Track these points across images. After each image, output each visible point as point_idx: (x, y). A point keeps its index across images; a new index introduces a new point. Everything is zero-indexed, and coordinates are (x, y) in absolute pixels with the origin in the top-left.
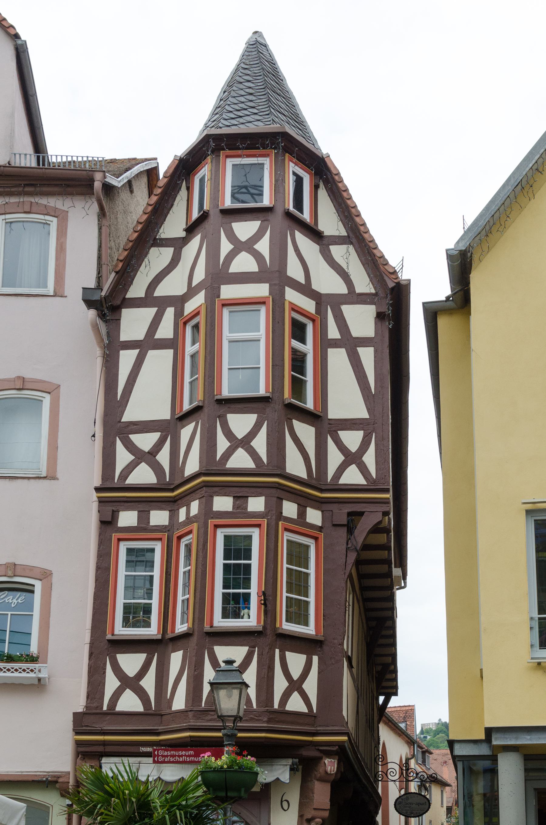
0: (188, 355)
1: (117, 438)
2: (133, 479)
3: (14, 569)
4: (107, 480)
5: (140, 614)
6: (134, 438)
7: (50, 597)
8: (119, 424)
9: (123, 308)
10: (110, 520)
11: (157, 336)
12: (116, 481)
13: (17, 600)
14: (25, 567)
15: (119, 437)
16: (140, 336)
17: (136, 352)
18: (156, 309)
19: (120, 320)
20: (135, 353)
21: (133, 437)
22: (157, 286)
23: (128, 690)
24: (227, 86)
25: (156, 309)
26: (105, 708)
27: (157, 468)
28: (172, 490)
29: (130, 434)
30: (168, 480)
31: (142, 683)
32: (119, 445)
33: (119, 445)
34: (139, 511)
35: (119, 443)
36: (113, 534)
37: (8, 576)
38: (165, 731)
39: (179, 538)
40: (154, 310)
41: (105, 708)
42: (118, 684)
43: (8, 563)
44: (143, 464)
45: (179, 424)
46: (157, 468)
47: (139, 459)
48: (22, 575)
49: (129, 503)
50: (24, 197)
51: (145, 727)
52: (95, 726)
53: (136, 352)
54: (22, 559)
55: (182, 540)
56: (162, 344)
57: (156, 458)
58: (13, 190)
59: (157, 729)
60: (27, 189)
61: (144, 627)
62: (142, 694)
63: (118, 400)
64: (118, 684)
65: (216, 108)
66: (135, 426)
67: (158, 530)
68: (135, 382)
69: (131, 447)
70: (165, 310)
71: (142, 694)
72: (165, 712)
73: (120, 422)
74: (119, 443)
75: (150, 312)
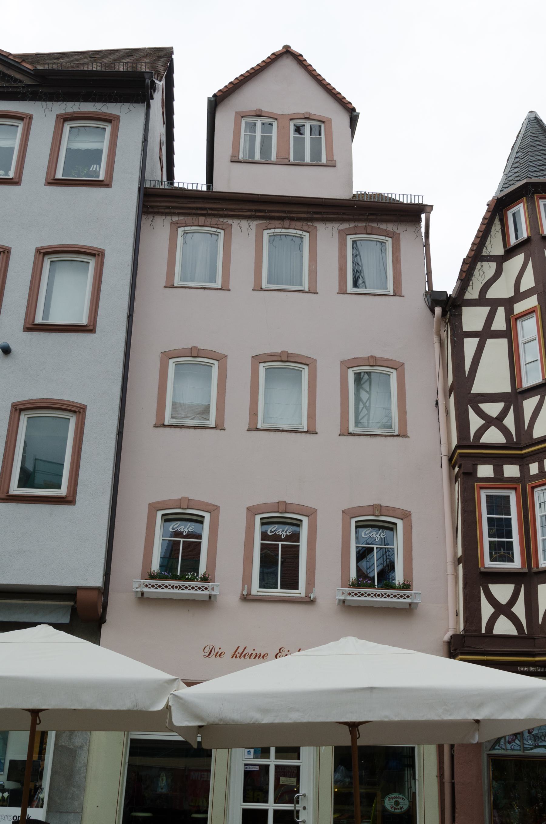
0: (522, 343)
1: (469, 406)
2: (486, 439)
3: (381, 510)
4: (464, 440)
5: (501, 550)
6: (483, 406)
7: (411, 533)
8: (470, 395)
9: (463, 307)
10: (472, 472)
11: (493, 328)
12: (471, 440)
13: (379, 536)
14: (389, 508)
15: (470, 406)
16: (479, 327)
17: (477, 340)
18: (489, 308)
19: (461, 315)
20: (475, 341)
21: (481, 405)
22: (487, 291)
23: (502, 616)
24: (519, 148)
25: (489, 308)
26: (483, 631)
27: (505, 431)
28: (521, 449)
29: (479, 403)
30: (515, 441)
31: (514, 610)
32: (471, 412)
33: (471, 412)
34: (493, 465)
35: (471, 411)
36: (476, 484)
37: (376, 516)
38: (543, 653)
39: (533, 488)
40: (488, 308)
41: (483, 631)
42: (493, 610)
43: (376, 505)
44: (493, 428)
45: (519, 397)
46: (505, 431)
47: (489, 423)
48: (387, 515)
49: (485, 459)
50: (369, 222)
51: (521, 649)
52: (476, 647)
53: (477, 340)
54: (386, 502)
55: (535, 490)
56: (498, 334)
57: (503, 422)
58: (360, 217)
59: (534, 651)
60: (370, 217)
61: (508, 562)
62: (514, 619)
63: (466, 376)
64: (493, 610)
65: (513, 163)
66: (482, 397)
67: (512, 481)
68: (479, 363)
69: (481, 414)
70: (497, 308)
71: (514, 619)
72: (539, 636)
73: (470, 393)
74: (471, 411)
75: (485, 310)
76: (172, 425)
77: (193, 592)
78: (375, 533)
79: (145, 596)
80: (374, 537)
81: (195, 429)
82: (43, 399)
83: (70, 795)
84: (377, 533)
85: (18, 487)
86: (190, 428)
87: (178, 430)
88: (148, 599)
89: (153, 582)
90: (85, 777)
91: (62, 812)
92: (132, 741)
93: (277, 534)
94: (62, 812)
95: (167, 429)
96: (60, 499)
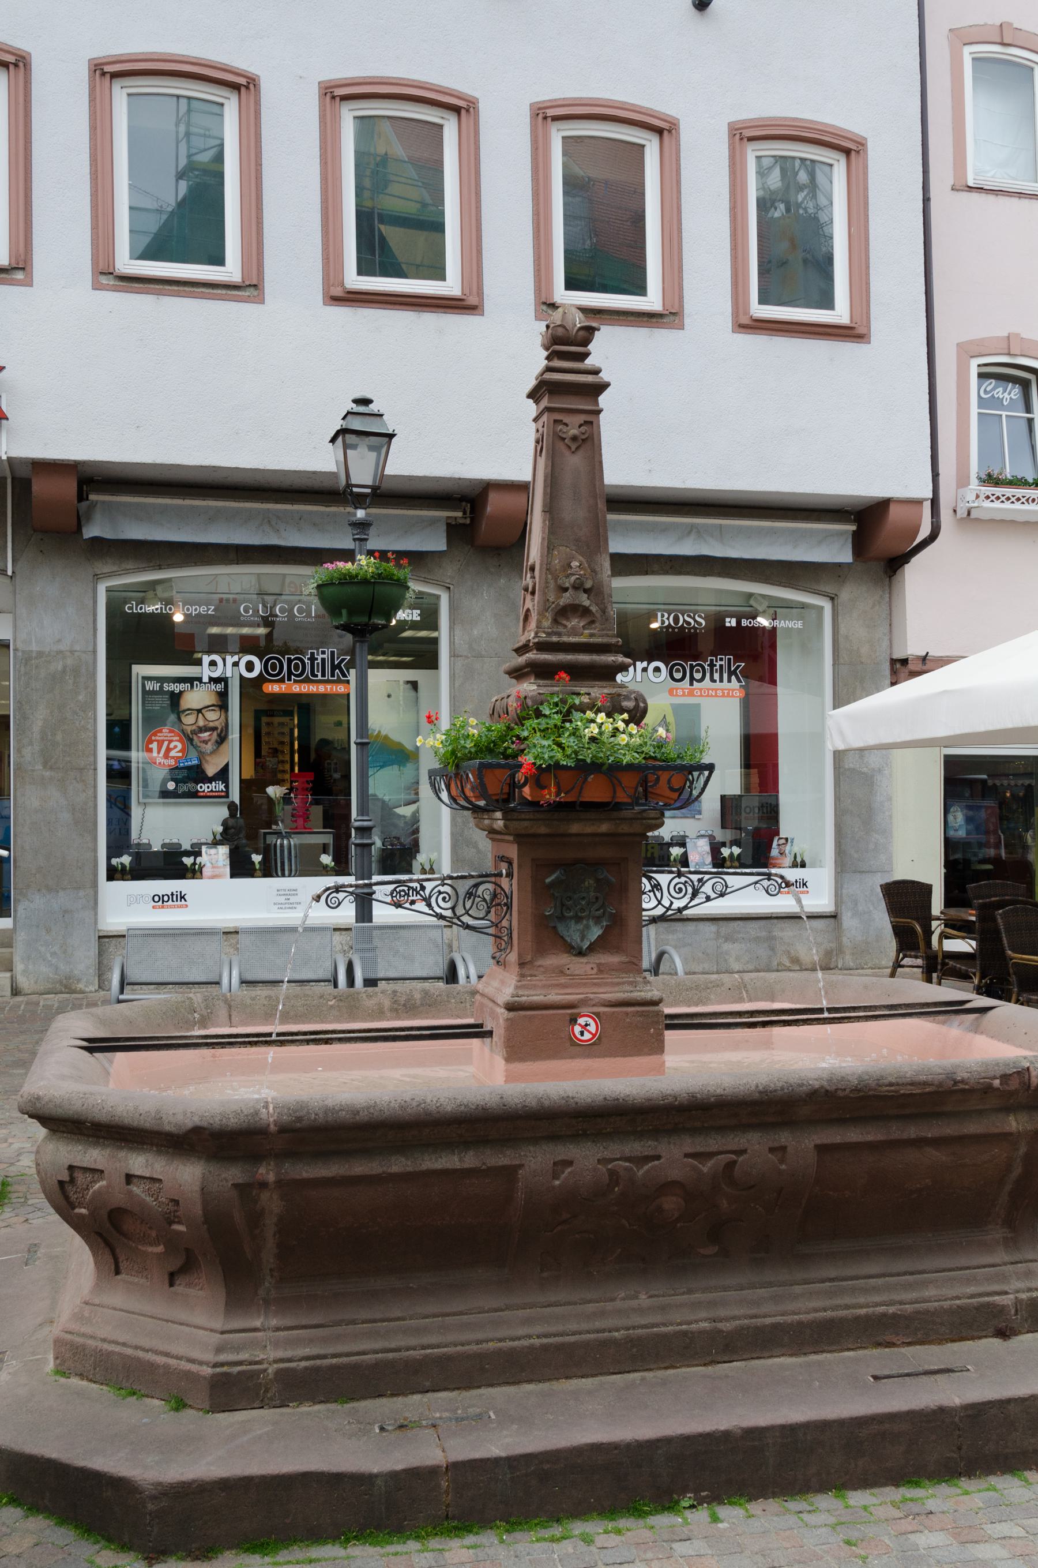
76: (982, 188)
77: (1007, 505)
78: (1001, 389)
79: (973, 515)
80: (1001, 397)
81: (1020, 198)
82: (785, 119)
83: (871, 846)
84: (1004, 391)
85: (444, 279)
86: (1011, 196)
87: (991, 198)
88: (977, 520)
89: (999, 491)
90: (891, 817)
91: (863, 872)
92: (946, 756)
93: (996, 396)
94: (863, 872)
95: (975, 196)
96: (786, 326)
